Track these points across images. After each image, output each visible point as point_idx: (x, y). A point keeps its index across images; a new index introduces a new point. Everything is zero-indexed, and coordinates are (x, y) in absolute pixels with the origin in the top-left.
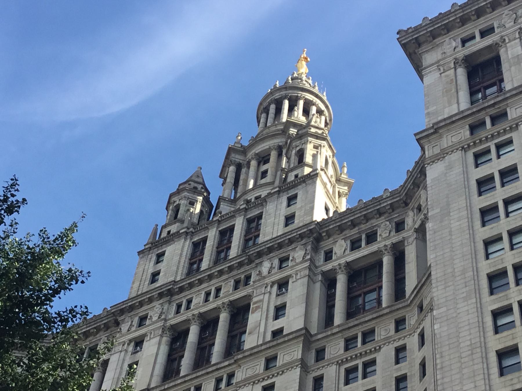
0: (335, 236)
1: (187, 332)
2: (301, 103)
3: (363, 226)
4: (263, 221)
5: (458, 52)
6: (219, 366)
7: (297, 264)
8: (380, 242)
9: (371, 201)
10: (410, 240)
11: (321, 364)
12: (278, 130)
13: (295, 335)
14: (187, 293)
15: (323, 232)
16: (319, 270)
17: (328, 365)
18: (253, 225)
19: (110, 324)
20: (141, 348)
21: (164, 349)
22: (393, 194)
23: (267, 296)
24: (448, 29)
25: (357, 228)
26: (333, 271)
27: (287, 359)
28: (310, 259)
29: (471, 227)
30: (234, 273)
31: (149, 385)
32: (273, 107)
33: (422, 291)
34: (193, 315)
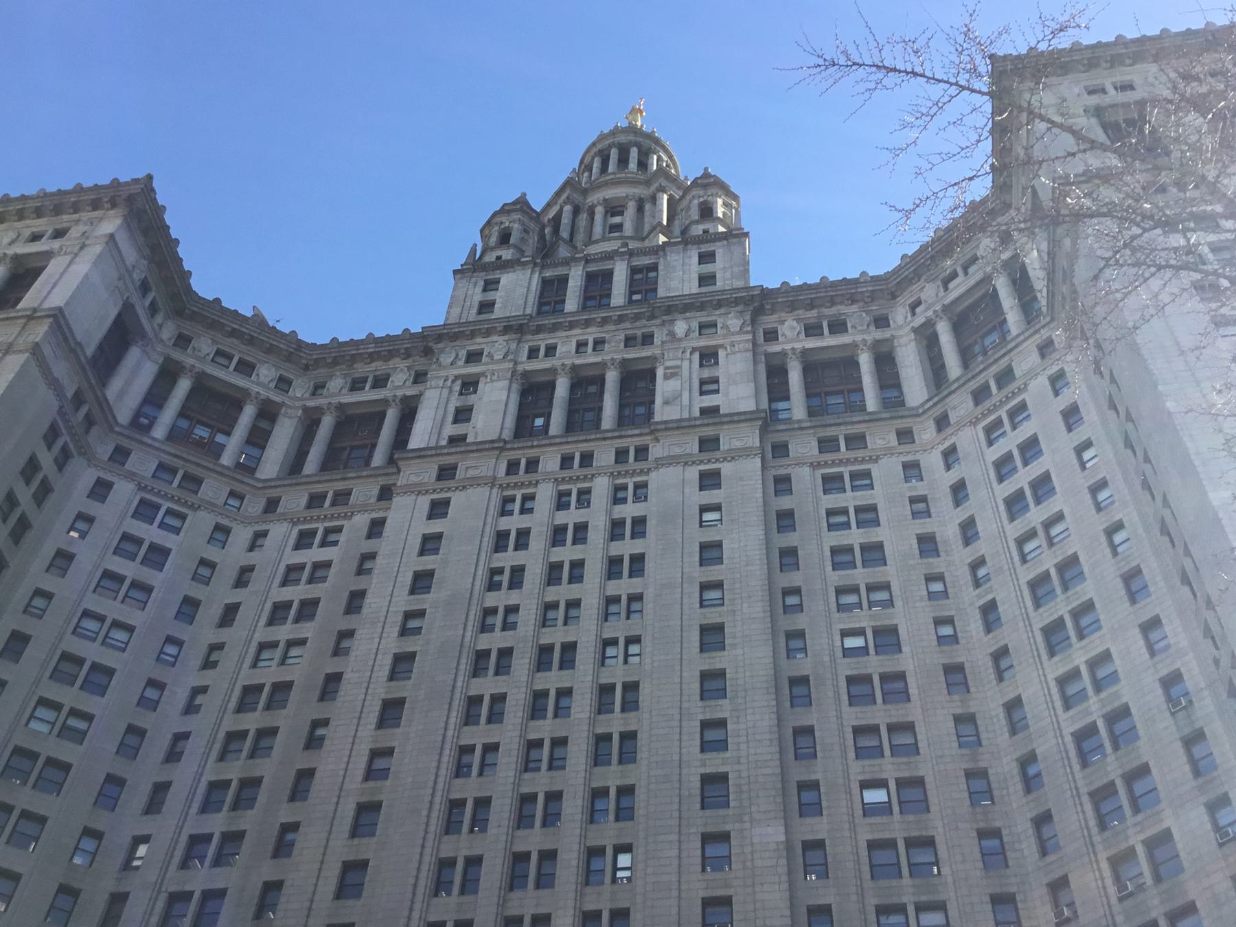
0: (783, 314)
10: (904, 340)
14: (547, 335)
22: (876, 279)
23: (686, 364)
30: (627, 325)
32: (614, 154)
33: (947, 400)
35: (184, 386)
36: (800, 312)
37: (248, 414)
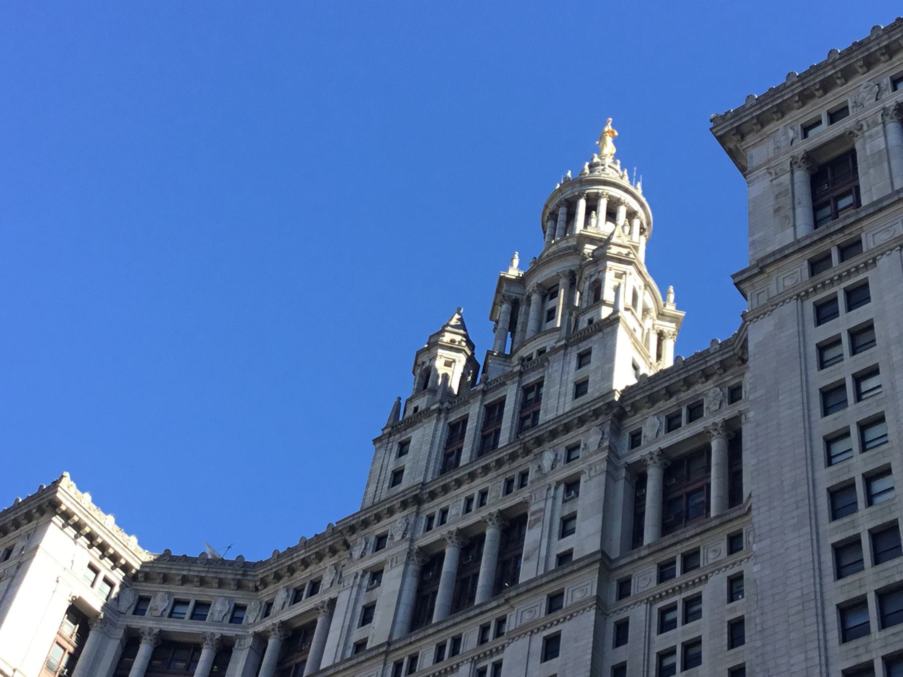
0: (645, 411)
1: (441, 555)
2: (603, 204)
3: (682, 394)
4: (543, 390)
5: (797, 147)
6: (484, 608)
7: (591, 455)
8: (706, 419)
9: (693, 357)
11: (626, 602)
12: (569, 248)
13: (588, 561)
14: (440, 499)
15: (627, 405)
16: (622, 462)
17: (635, 604)
18: (531, 397)
19: (338, 546)
20: (380, 582)
21: (411, 583)
22: (725, 345)
23: (550, 502)
24: (781, 111)
25: (674, 399)
26: (642, 463)
27: (578, 596)
28: (609, 448)
29: (807, 417)
30: (505, 468)
31: (391, 636)
32: (562, 211)
34: (450, 532)
35: (144, 650)
36: (660, 404)
37: (205, 655)
